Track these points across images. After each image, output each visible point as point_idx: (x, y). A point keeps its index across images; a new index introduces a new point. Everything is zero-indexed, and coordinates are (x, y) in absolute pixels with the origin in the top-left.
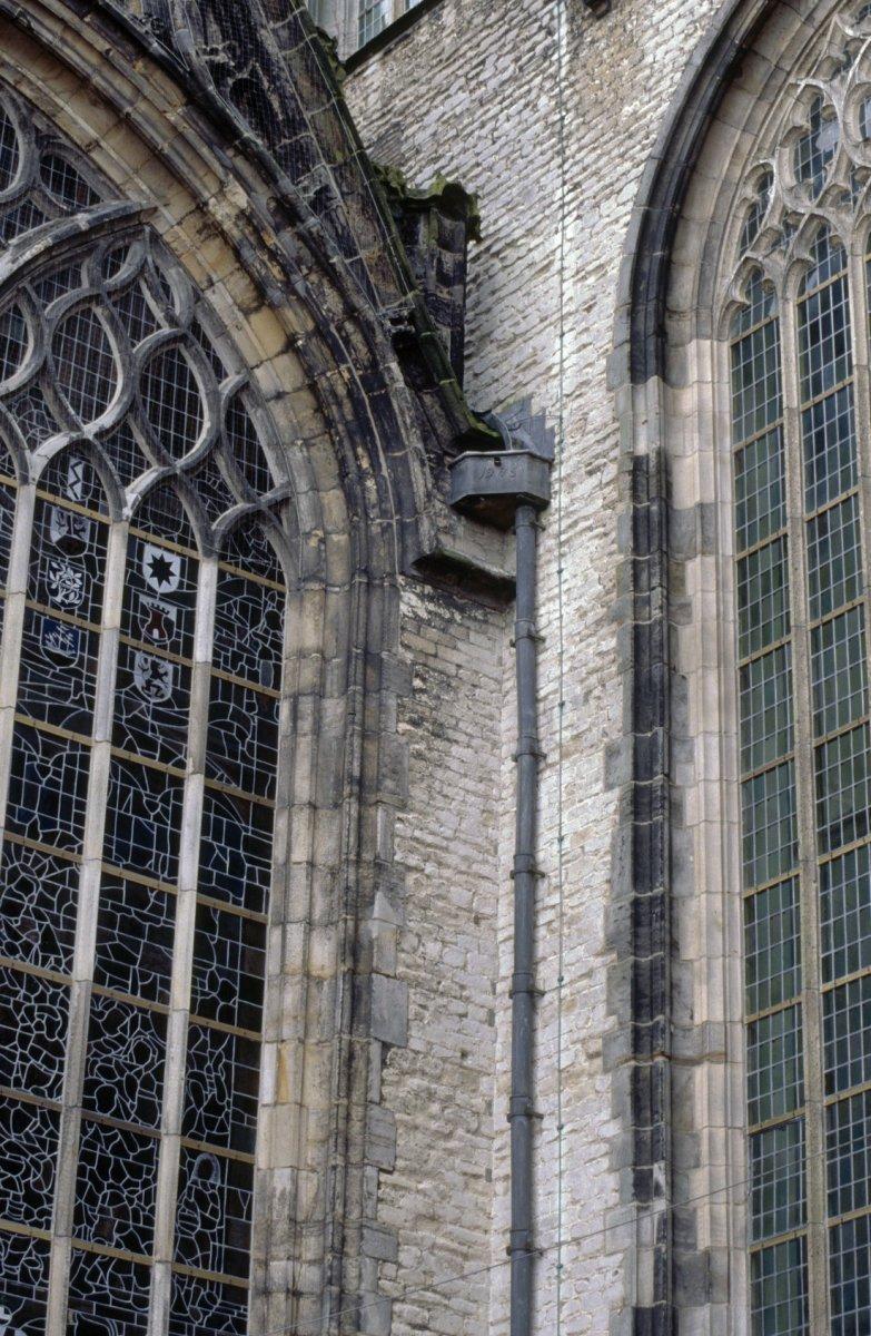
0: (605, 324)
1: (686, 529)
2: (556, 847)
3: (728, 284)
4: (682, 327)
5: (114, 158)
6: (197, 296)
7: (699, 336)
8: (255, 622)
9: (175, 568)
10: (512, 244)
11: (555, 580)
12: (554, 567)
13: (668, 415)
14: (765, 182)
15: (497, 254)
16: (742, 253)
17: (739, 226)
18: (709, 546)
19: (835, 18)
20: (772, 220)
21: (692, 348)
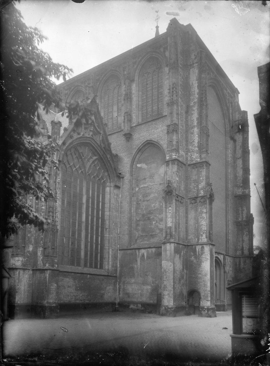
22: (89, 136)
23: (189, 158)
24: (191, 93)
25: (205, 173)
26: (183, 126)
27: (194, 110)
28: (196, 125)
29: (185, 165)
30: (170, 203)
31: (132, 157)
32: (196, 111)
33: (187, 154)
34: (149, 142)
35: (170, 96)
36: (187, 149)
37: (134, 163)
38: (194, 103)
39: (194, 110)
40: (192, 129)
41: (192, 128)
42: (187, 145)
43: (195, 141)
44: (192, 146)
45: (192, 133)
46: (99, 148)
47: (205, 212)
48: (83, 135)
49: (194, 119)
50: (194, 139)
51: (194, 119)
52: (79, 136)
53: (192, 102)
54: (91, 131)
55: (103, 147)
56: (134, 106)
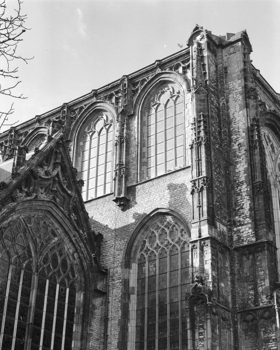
0: (120, 257)
1: (130, 290)
2: (110, 332)
3: (138, 256)
4: (131, 261)
5: (60, 231)
6: (68, 249)
7: (134, 263)
8: (72, 297)
9: (64, 290)
10: (107, 241)
11: (111, 294)
12: (111, 292)
13: (129, 273)
14: (145, 242)
15: (104, 242)
16: (140, 252)
17: (140, 248)
18: (133, 294)
19: (157, 222)
20: (145, 249)
21: (133, 264)
22: (48, 200)
23: (235, 238)
24: (233, 130)
25: (267, 264)
26: (220, 182)
27: (239, 157)
28: (244, 179)
29: (227, 248)
30: (201, 321)
31: (130, 237)
32: (243, 157)
33: (230, 230)
34: (159, 211)
35: (195, 128)
36: (229, 221)
37: (131, 249)
38: (238, 145)
39: (239, 157)
40: (237, 187)
41: (238, 185)
42: (230, 214)
43: (244, 206)
44: (240, 216)
45: (239, 194)
46: (67, 221)
47: (273, 338)
48: (36, 197)
49: (240, 172)
50: (243, 204)
51: (240, 172)
52: (29, 198)
53: (235, 143)
54: (52, 191)
55: (73, 219)
56: (133, 153)
